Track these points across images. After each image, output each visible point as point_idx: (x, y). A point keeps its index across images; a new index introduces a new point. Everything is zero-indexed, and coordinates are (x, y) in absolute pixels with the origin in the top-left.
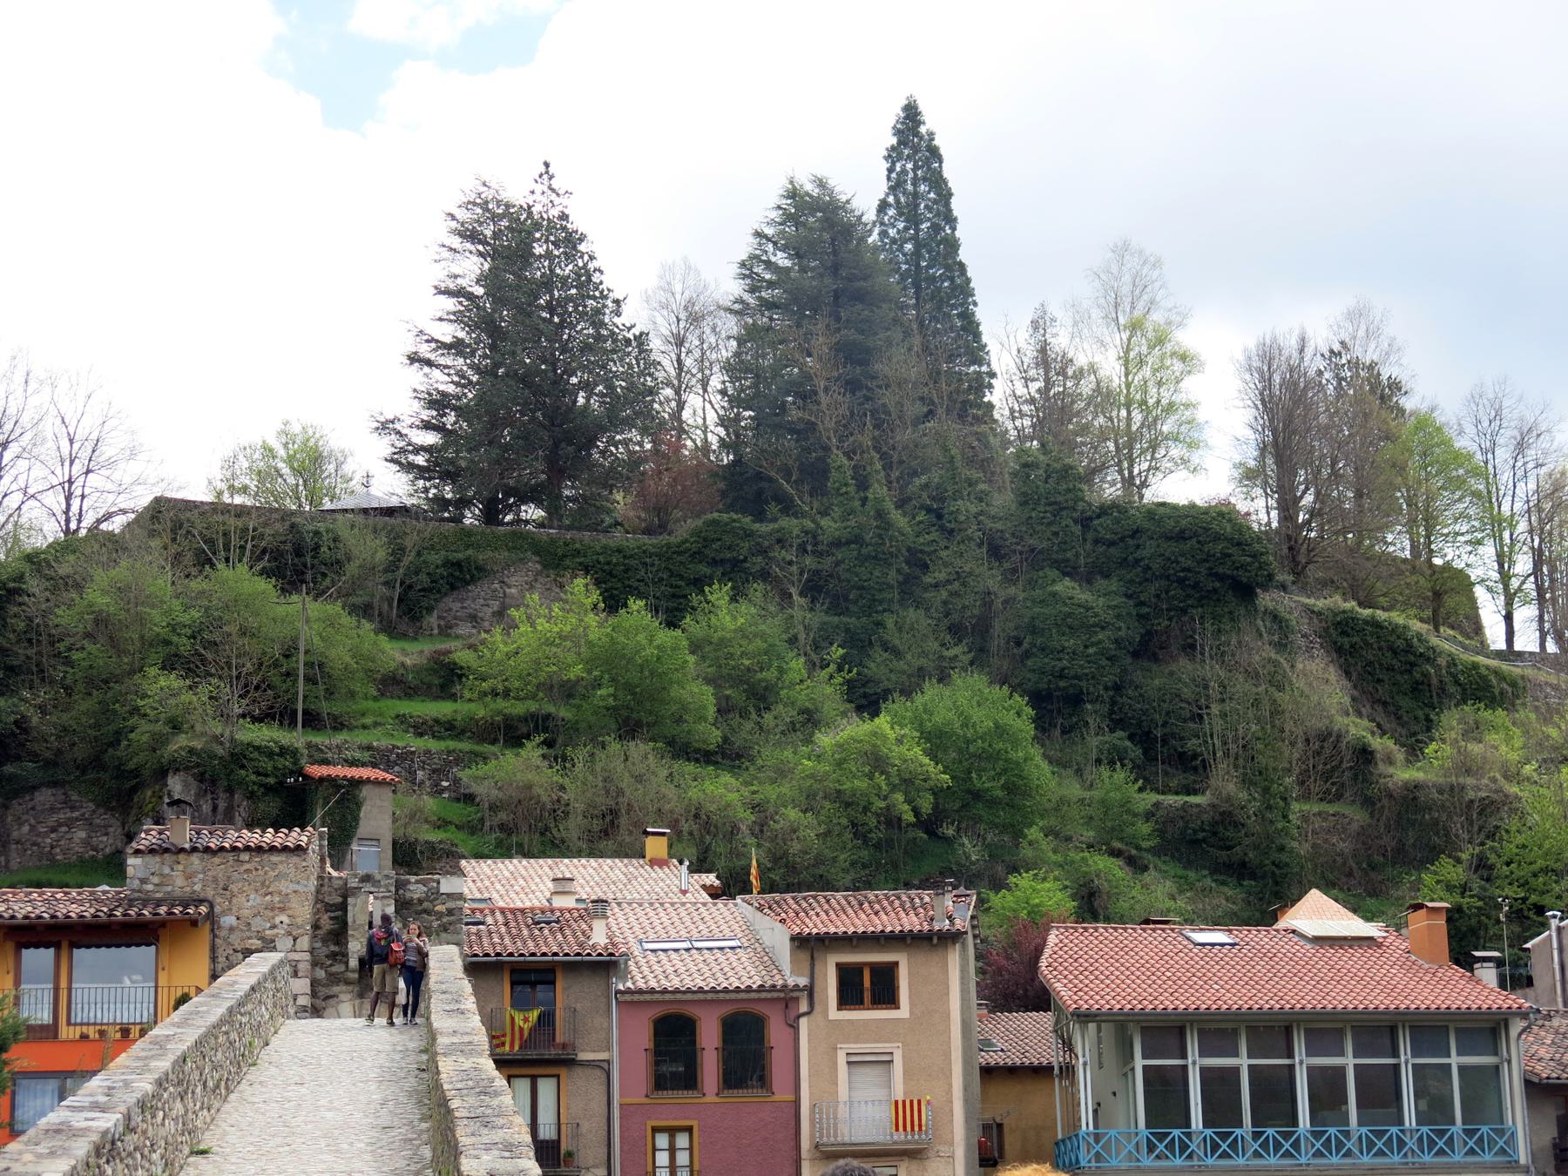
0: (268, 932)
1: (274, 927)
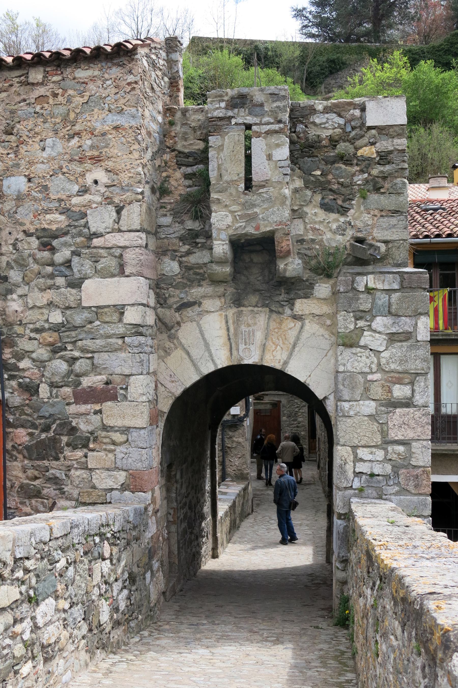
0: (75, 200)
1: (84, 191)
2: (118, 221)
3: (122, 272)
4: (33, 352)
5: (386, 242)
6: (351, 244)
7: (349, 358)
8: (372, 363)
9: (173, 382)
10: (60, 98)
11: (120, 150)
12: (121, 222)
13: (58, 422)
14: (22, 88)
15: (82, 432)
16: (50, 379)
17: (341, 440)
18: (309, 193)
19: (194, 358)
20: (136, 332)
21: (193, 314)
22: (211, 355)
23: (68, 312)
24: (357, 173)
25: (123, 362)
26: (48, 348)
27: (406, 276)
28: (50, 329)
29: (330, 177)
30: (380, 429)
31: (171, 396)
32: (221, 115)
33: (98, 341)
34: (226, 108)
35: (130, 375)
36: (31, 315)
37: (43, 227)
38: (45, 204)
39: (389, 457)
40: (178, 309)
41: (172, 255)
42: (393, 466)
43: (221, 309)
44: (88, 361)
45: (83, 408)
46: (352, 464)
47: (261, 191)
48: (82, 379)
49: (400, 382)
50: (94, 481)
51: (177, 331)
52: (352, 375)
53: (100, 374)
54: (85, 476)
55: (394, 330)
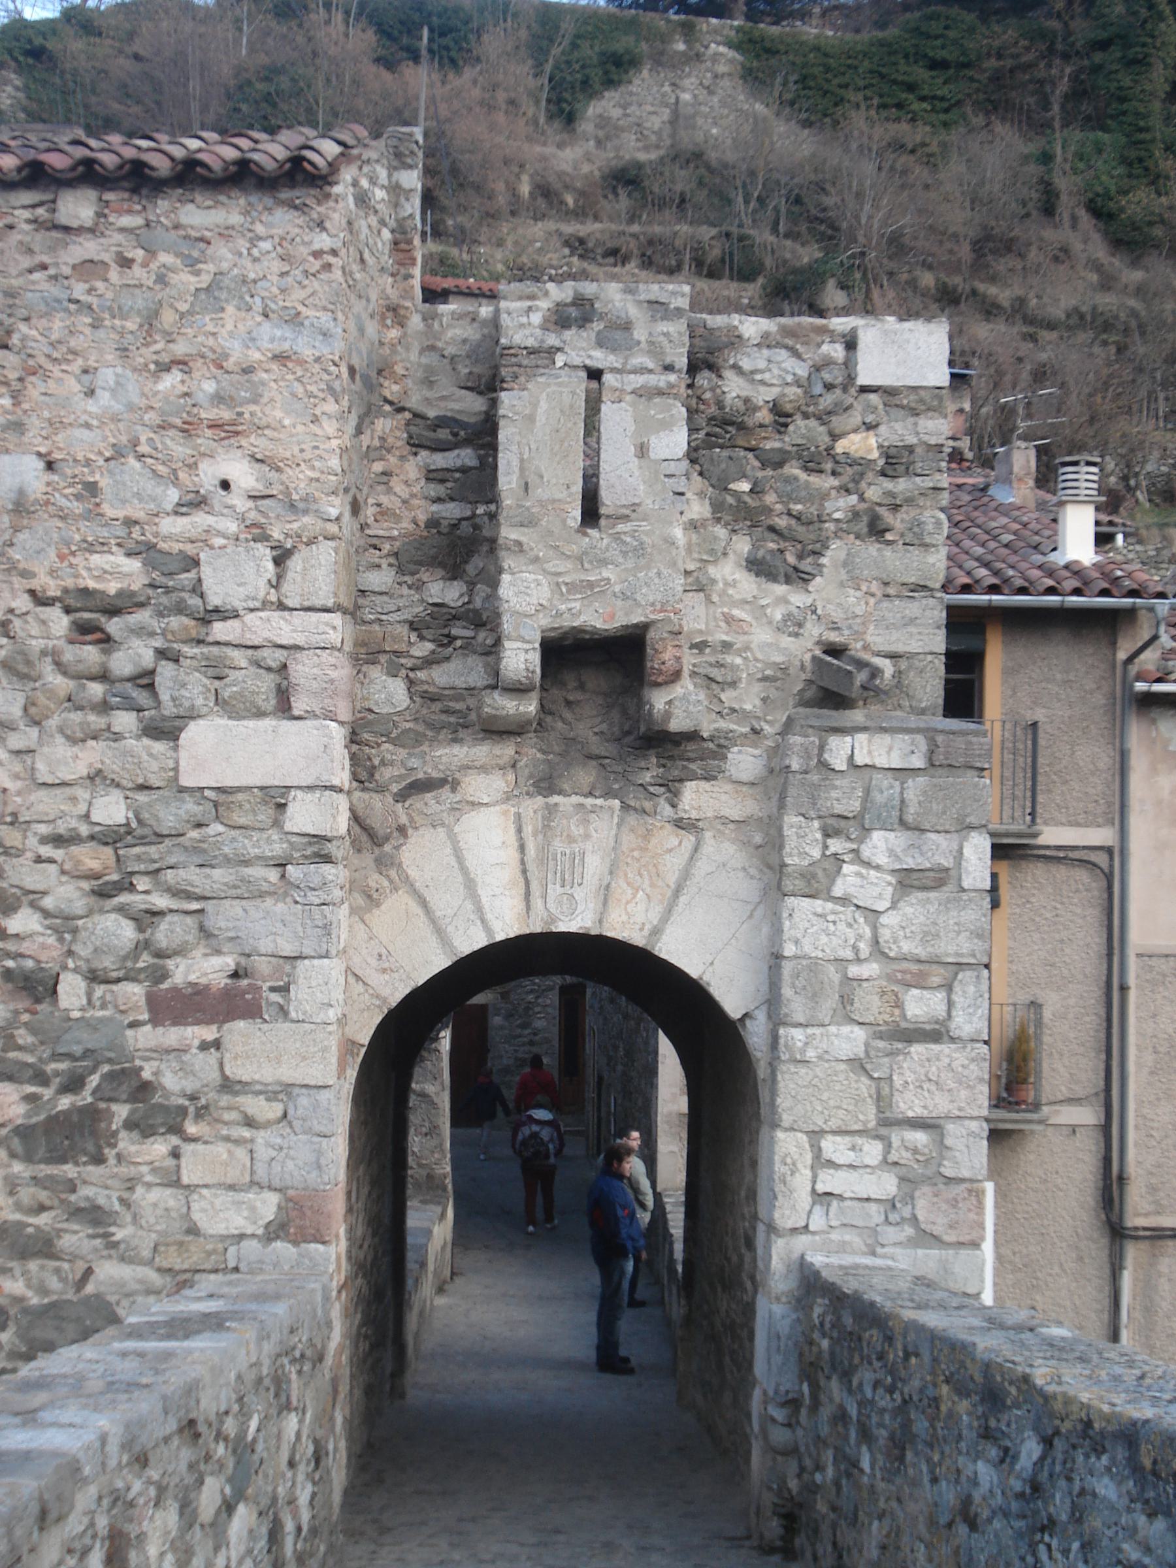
1: (196, 502)
2: (276, 584)
3: (284, 706)
4: (44, 893)
5: (893, 656)
6: (814, 658)
7: (807, 925)
8: (860, 937)
9: (384, 971)
10: (137, 271)
11: (287, 413)
12: (286, 587)
13: (106, 1068)
14: (39, 237)
15: (167, 1094)
16: (88, 961)
17: (785, 1117)
18: (721, 532)
19: (438, 914)
20: (317, 855)
21: (438, 808)
22: (479, 910)
23: (142, 798)
24: (833, 493)
25: (278, 925)
26: (86, 885)
27: (940, 739)
28: (92, 837)
29: (770, 498)
30: (873, 1091)
31: (379, 1007)
32: (530, 342)
33: (217, 873)
34: (544, 328)
35: (300, 957)
36: (45, 803)
37: (82, 584)
38: (90, 531)
39: (893, 1157)
40: (401, 797)
41: (391, 662)
42: (902, 1179)
43: (508, 798)
44: (189, 920)
45: (173, 1037)
46: (808, 1173)
47: (621, 527)
48: (170, 963)
49: (919, 981)
50: (196, 1216)
51: (397, 848)
52: (814, 966)
53: (218, 952)
54: (172, 1203)
55: (910, 863)
